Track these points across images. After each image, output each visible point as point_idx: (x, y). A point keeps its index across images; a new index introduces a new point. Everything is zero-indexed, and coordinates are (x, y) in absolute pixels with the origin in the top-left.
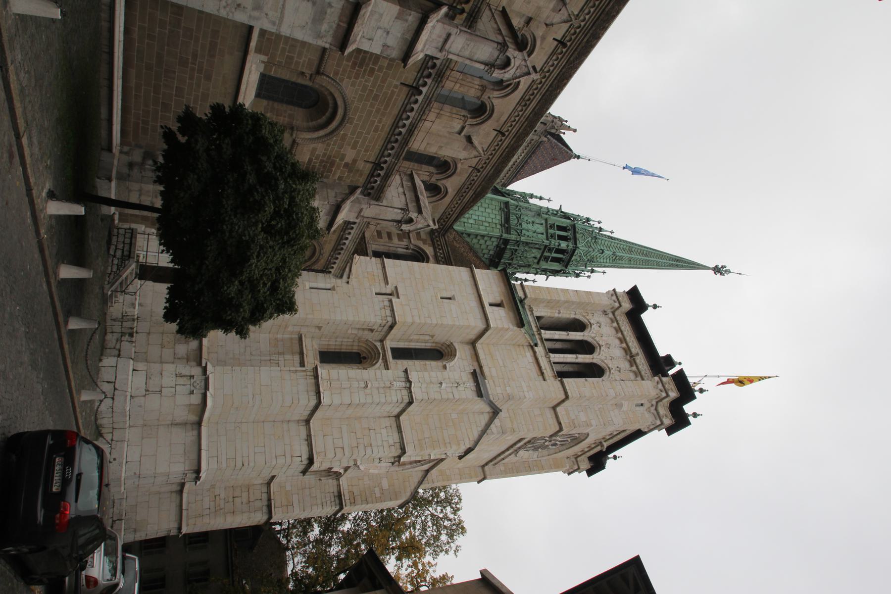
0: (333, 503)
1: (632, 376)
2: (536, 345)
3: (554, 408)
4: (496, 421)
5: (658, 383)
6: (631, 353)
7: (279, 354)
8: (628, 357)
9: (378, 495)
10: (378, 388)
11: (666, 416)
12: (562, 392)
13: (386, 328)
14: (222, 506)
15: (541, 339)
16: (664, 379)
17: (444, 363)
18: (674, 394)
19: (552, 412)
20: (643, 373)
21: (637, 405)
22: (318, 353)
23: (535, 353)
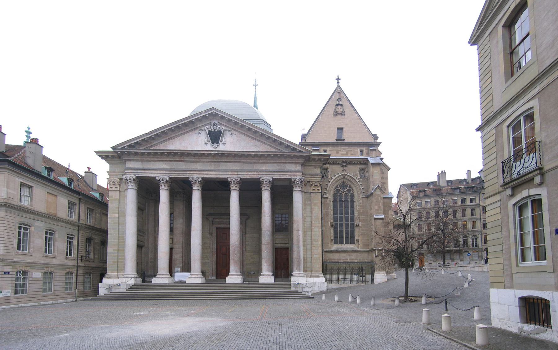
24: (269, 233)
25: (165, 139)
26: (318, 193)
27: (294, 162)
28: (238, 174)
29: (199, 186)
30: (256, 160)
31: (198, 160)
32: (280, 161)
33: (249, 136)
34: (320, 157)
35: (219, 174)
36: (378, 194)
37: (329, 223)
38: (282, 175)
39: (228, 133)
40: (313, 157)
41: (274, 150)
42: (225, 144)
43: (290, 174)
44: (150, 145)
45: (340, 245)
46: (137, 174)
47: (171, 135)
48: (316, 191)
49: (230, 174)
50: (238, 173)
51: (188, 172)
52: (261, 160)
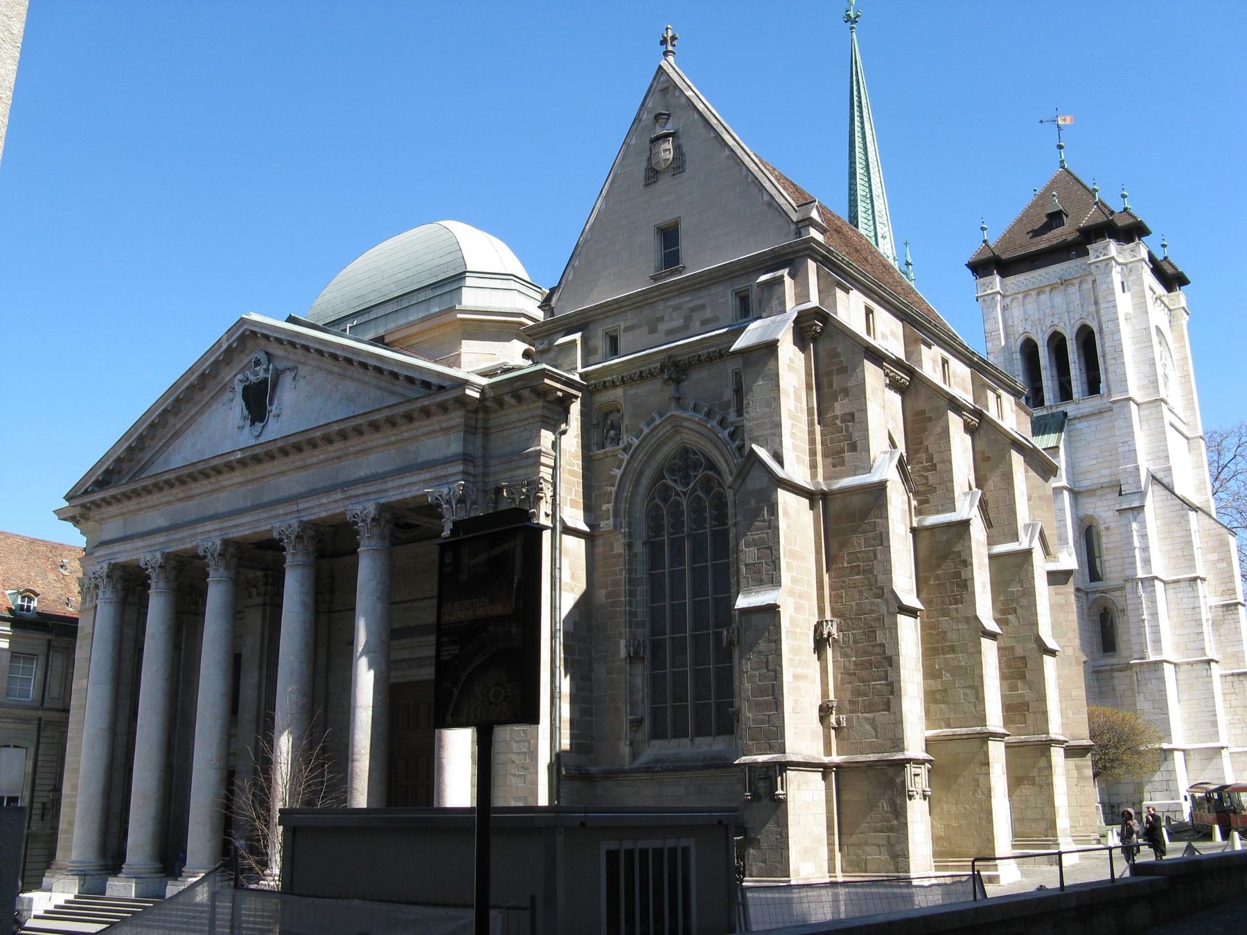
0: (1235, 612)
1: (1088, 286)
2: (1065, 414)
3: (1138, 405)
4: (1159, 476)
6: (1057, 283)
7: (1114, 690)
8: (1062, 288)
12: (1125, 403)
13: (1079, 594)
14: (1239, 717)
15: (1057, 406)
17: (1102, 527)
18: (1113, 247)
21: (1124, 291)
22: (1106, 654)
23: (1075, 418)
25: (164, 441)
27: (437, 427)
29: (221, 569)
32: (399, 438)
33: (331, 372)
37: (623, 642)
38: (409, 484)
39: (287, 379)
41: (392, 400)
42: (278, 416)
43: (428, 476)
44: (138, 467)
49: (284, 515)
50: (302, 506)
51: (199, 530)
52: (352, 446)
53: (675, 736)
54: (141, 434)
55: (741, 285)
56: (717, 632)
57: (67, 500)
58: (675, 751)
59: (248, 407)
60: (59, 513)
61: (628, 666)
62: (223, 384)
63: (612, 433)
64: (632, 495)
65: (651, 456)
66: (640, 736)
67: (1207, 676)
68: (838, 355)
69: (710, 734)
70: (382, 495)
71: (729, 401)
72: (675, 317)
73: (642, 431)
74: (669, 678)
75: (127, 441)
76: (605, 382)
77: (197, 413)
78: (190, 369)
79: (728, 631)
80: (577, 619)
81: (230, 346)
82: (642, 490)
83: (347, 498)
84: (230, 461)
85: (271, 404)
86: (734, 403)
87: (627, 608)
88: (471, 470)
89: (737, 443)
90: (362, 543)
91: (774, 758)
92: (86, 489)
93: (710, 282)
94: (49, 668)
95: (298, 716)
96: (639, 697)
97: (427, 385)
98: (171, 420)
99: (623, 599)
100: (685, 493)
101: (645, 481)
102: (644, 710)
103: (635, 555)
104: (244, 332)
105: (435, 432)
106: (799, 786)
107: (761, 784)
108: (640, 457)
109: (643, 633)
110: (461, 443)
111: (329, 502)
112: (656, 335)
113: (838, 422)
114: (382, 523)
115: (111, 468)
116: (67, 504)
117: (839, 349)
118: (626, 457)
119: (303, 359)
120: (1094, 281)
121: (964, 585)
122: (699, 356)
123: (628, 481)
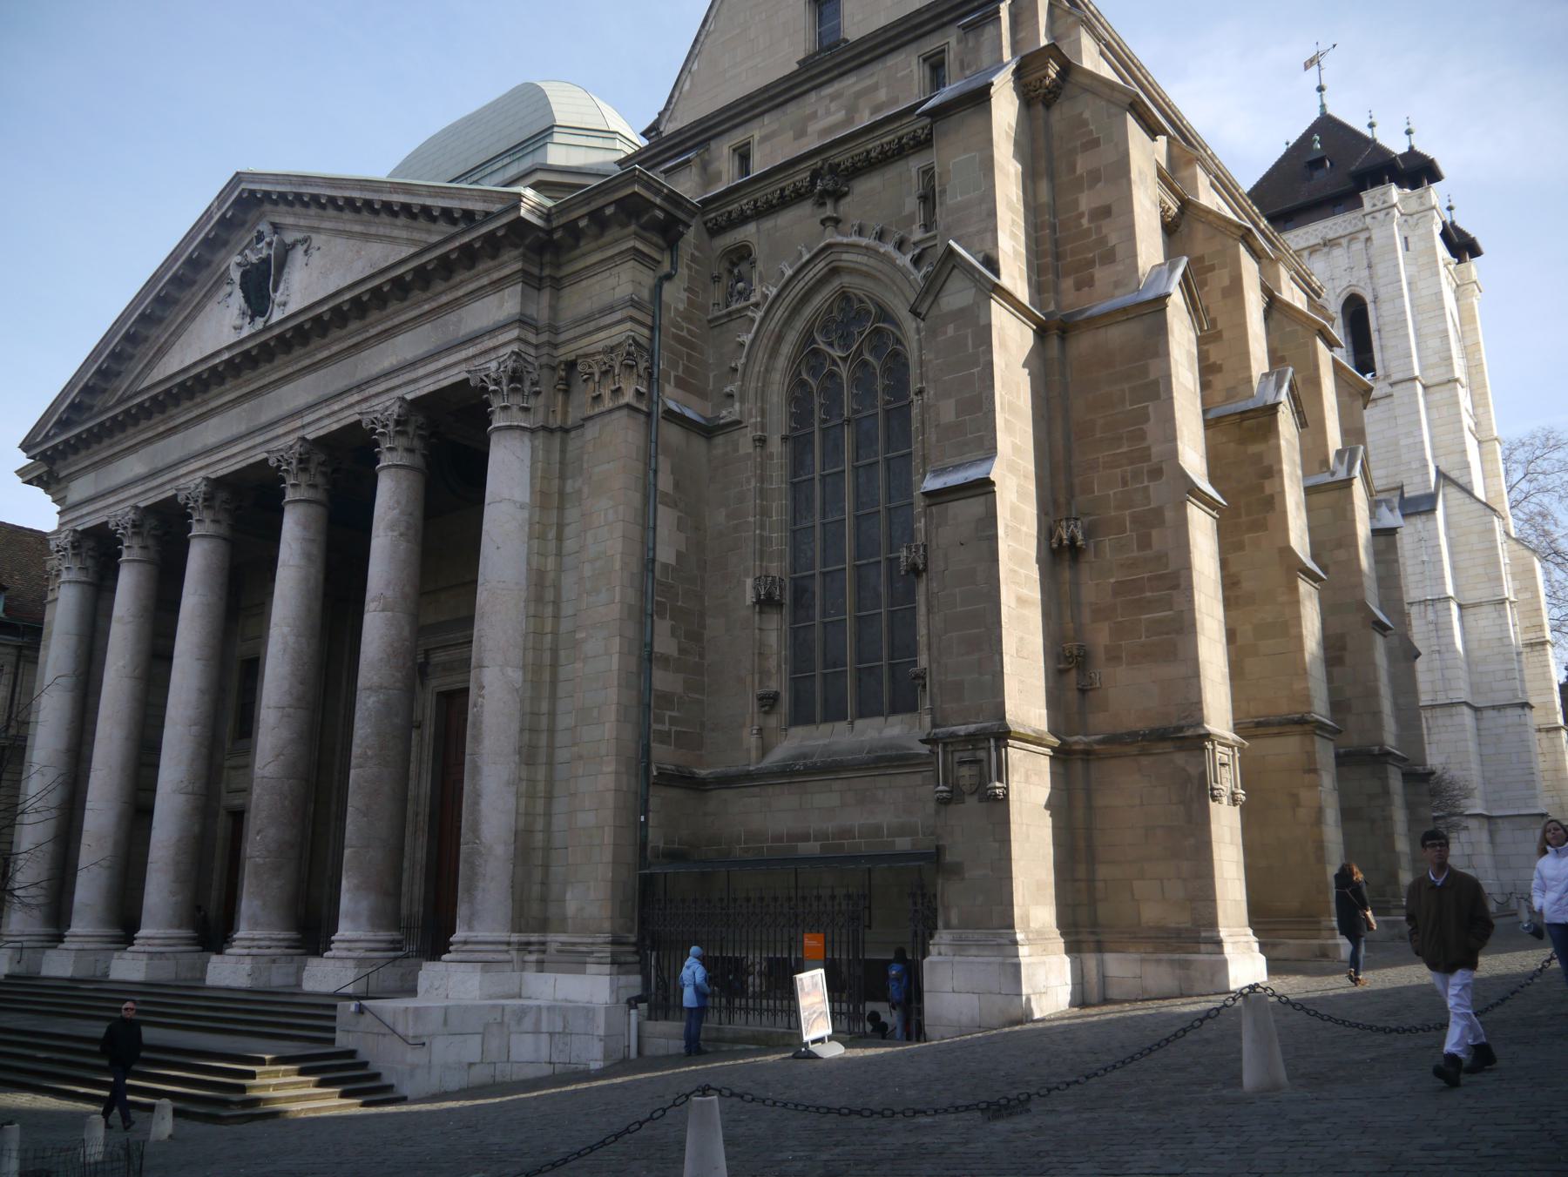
0: (1542, 652)
1: (1358, 246)
4: (1454, 474)
5: (1374, 218)
6: (1319, 244)
8: (1326, 250)
9: (1528, 595)
10: (1438, 637)
11: (1420, 197)
12: (1409, 384)
14: (1549, 783)
16: (1367, 207)
18: (1395, 193)
19: (1432, 390)
20: (1350, 229)
21: (1407, 249)
24: (371, 701)
25: (145, 362)
26: (617, 415)
27: (485, 281)
28: (303, 427)
29: (207, 521)
30: (357, 332)
31: (204, 409)
32: (434, 304)
33: (350, 235)
34: (594, 205)
35: (254, 447)
36: (962, 310)
37: (749, 582)
38: (446, 368)
40: (563, 220)
43: (471, 351)
45: (822, 727)
46: (79, 522)
47: (158, 337)
48: (608, 404)
50: (308, 419)
52: (372, 325)
53: (827, 719)
54: (113, 350)
55: (931, 44)
56: (890, 560)
57: (24, 450)
58: (826, 741)
59: (247, 299)
60: (21, 472)
61: (757, 617)
62: (219, 274)
63: (740, 285)
64: (767, 370)
65: (795, 311)
66: (773, 721)
67: (1520, 725)
68: (1085, 123)
69: (880, 713)
70: (411, 387)
71: (914, 213)
72: (833, 109)
73: (783, 273)
74: (818, 632)
75: (96, 362)
76: (730, 213)
77: (186, 318)
78: (172, 254)
79: (909, 548)
80: (683, 549)
81: (224, 215)
82: (782, 362)
83: (365, 400)
84: (215, 366)
85: (275, 290)
86: (920, 218)
87: (758, 532)
88: (532, 338)
89: (924, 271)
90: (382, 458)
91: (985, 728)
92: (48, 432)
93: (887, 48)
94: (19, 683)
95: (291, 710)
96: (772, 663)
97: (468, 215)
98: (154, 332)
99: (751, 519)
100: (844, 359)
101: (786, 349)
102: (778, 683)
103: (771, 456)
104: (241, 194)
105: (484, 286)
106: (1027, 777)
107: (965, 771)
108: (779, 313)
109: (777, 568)
110: (518, 299)
111: (342, 410)
112: (804, 140)
113: (1085, 222)
114: (410, 429)
115: (77, 400)
116: (23, 460)
117: (1087, 115)
118: (758, 315)
119: (316, 223)
120: (1368, 239)
121: (1272, 504)
122: (868, 152)
123: (762, 349)
